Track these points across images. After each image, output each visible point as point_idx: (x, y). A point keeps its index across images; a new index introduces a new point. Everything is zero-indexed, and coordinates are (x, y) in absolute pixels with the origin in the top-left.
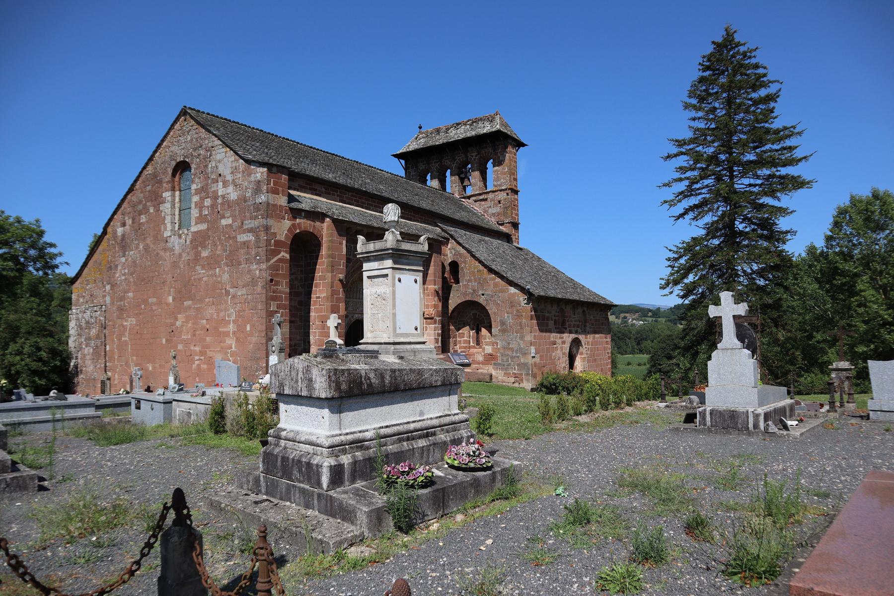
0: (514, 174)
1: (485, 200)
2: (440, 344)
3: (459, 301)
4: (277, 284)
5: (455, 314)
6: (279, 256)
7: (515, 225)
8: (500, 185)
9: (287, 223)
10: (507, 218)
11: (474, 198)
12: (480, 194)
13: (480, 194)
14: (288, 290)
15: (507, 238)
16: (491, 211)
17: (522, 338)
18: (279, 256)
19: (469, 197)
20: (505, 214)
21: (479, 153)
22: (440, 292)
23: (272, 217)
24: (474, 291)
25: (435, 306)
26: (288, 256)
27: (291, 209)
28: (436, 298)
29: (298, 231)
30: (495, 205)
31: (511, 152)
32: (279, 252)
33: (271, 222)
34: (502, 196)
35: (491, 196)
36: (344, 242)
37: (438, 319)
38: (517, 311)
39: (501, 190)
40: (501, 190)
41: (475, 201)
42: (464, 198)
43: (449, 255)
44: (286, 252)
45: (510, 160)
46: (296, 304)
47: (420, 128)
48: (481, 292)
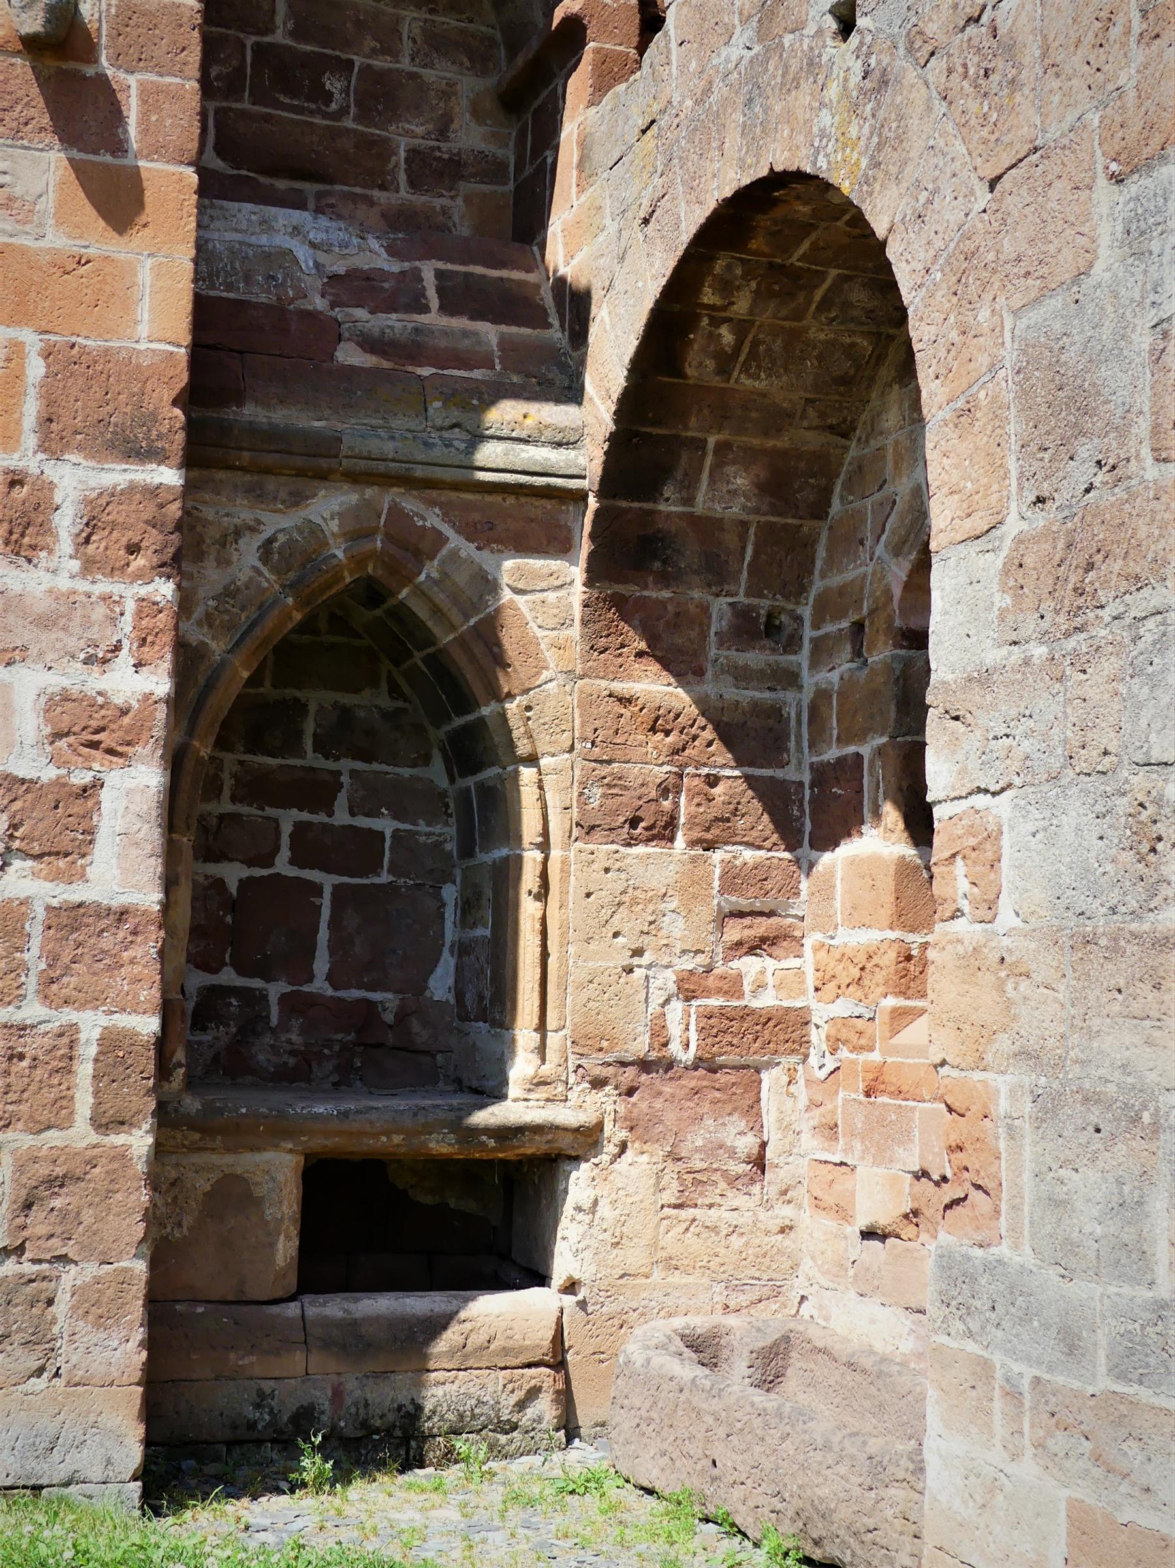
37: (74, 480)
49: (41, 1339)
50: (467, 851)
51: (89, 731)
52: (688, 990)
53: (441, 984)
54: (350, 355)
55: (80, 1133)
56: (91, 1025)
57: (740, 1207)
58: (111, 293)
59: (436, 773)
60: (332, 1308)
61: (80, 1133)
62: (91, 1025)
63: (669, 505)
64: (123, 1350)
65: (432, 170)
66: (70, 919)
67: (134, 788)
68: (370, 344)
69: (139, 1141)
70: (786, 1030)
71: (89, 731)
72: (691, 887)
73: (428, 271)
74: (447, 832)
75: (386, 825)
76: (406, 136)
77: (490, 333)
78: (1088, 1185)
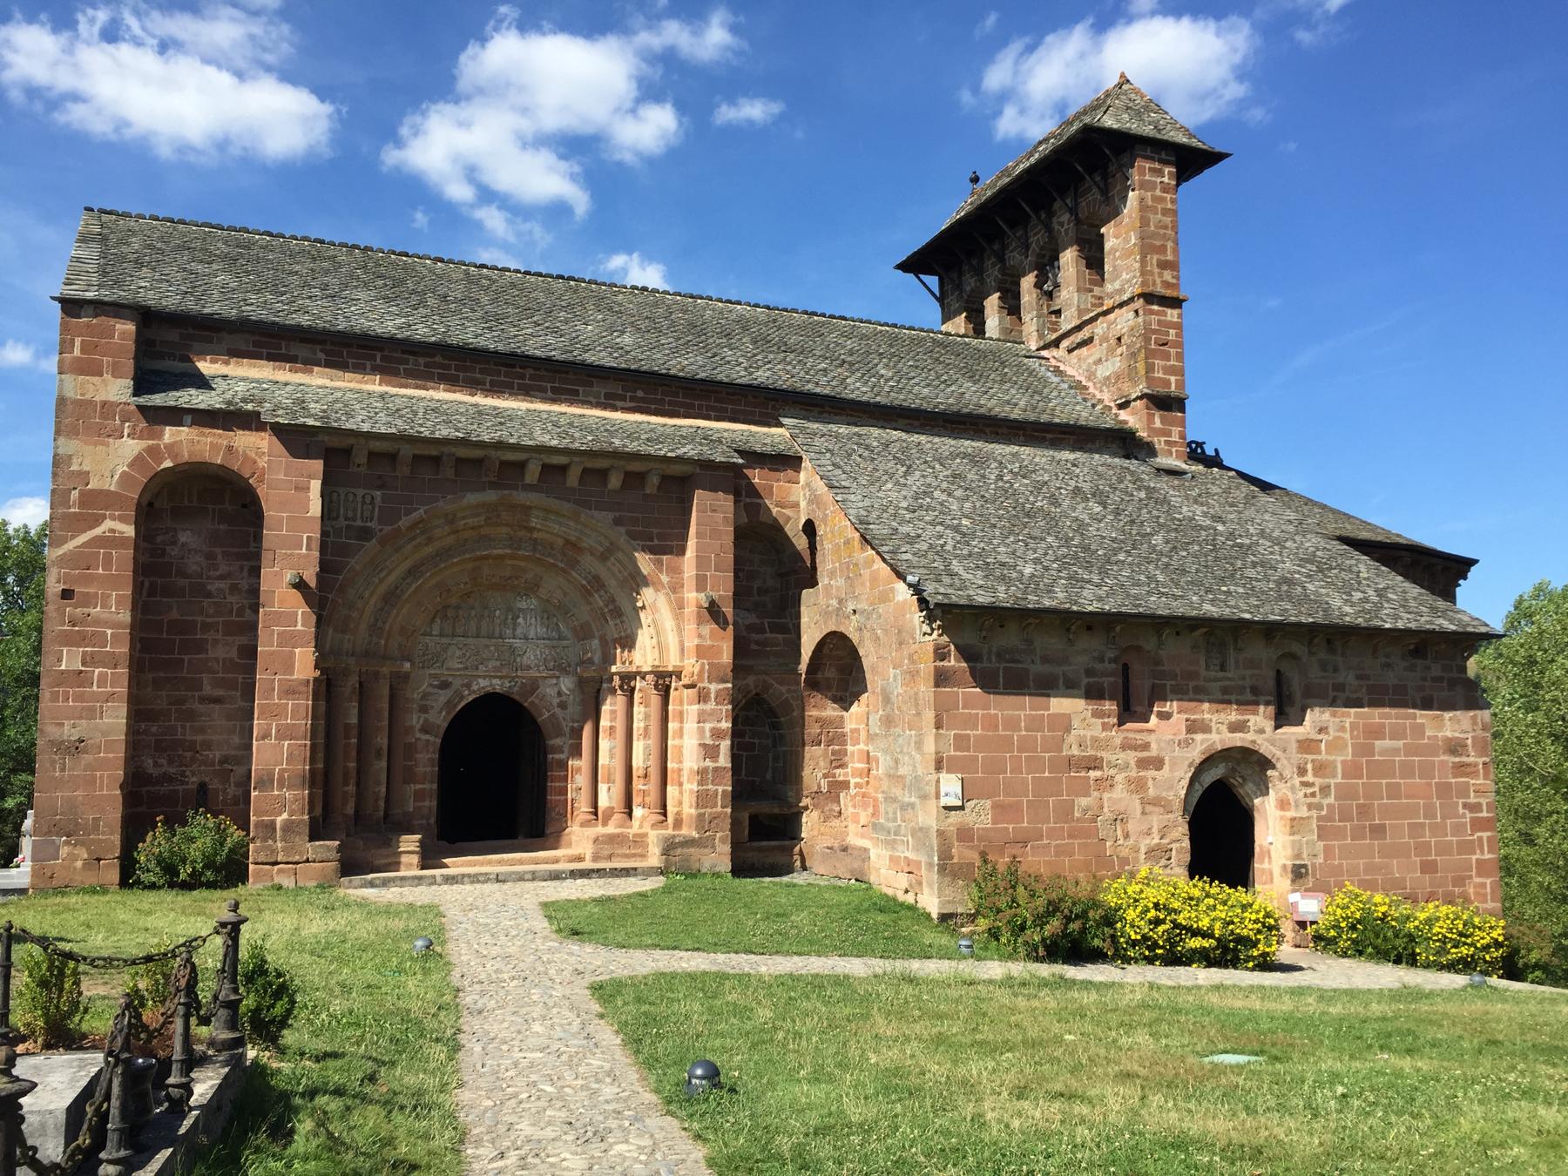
0: (1162, 249)
1: (1087, 342)
2: (724, 760)
3: (818, 637)
4: (89, 601)
5: (830, 673)
6: (98, 531)
7: (1167, 403)
8: (1121, 291)
9: (129, 447)
10: (1136, 384)
11: (1065, 344)
12: (1078, 328)
13: (1078, 328)
14: (126, 616)
15: (1126, 443)
16: (1104, 371)
17: (919, 745)
18: (98, 531)
19: (1056, 344)
20: (1131, 375)
21: (1073, 211)
22: (728, 610)
23: (73, 432)
24: (840, 601)
25: (701, 652)
26: (129, 530)
27: (141, 408)
28: (709, 628)
29: (168, 464)
30: (1111, 351)
31: (1144, 185)
32: (98, 521)
33: (68, 446)
34: (1124, 320)
35: (1100, 328)
36: (316, 485)
37: (713, 687)
38: (910, 657)
39: (1121, 305)
40: (1121, 305)
41: (1070, 351)
42: (1045, 347)
43: (803, 504)
44: (122, 519)
45: (1143, 207)
46: (234, 654)
47: (975, 180)
48: (851, 606)
49: (713, 846)
50: (774, 746)
51: (717, 734)
52: (825, 776)
53: (769, 776)
54: (754, 647)
55: (719, 809)
56: (720, 789)
57: (835, 822)
58: (719, 651)
59: (767, 729)
60: (756, 844)
61: (719, 809)
62: (720, 789)
63: (819, 675)
64: (727, 848)
65: (762, 592)
66: (716, 769)
67: (725, 745)
68: (757, 643)
69: (729, 810)
70: (845, 785)
71: (717, 734)
72: (825, 755)
73: (766, 621)
74: (770, 742)
75: (756, 741)
76: (756, 584)
77: (780, 636)
78: (890, 810)
